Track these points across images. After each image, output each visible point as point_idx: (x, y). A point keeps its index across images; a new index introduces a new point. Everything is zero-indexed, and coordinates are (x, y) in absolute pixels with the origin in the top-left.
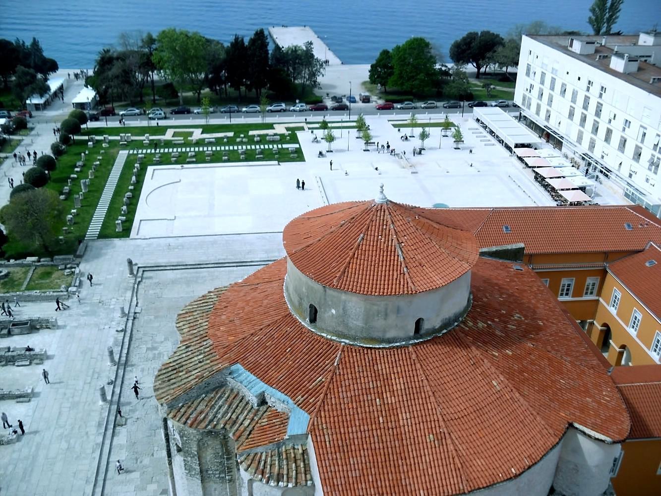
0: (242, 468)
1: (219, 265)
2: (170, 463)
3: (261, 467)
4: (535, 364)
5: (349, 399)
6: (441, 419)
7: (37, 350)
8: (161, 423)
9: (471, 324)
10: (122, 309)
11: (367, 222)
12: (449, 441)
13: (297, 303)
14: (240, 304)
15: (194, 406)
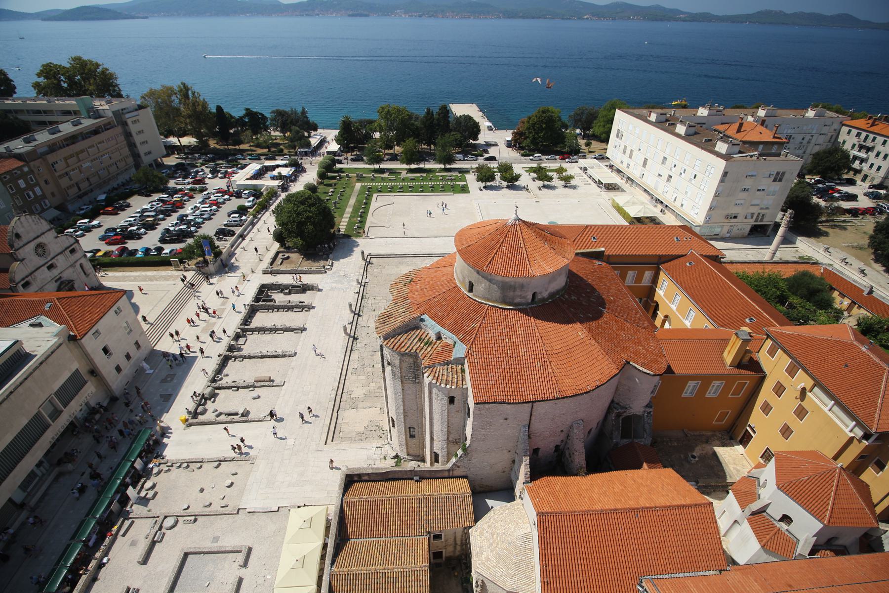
0: (426, 375)
1: (415, 256)
2: (384, 371)
3: (437, 375)
4: (607, 324)
6: (545, 353)
7: (306, 303)
9: (567, 297)
10: (357, 280)
12: (549, 367)
13: (461, 280)
14: (428, 280)
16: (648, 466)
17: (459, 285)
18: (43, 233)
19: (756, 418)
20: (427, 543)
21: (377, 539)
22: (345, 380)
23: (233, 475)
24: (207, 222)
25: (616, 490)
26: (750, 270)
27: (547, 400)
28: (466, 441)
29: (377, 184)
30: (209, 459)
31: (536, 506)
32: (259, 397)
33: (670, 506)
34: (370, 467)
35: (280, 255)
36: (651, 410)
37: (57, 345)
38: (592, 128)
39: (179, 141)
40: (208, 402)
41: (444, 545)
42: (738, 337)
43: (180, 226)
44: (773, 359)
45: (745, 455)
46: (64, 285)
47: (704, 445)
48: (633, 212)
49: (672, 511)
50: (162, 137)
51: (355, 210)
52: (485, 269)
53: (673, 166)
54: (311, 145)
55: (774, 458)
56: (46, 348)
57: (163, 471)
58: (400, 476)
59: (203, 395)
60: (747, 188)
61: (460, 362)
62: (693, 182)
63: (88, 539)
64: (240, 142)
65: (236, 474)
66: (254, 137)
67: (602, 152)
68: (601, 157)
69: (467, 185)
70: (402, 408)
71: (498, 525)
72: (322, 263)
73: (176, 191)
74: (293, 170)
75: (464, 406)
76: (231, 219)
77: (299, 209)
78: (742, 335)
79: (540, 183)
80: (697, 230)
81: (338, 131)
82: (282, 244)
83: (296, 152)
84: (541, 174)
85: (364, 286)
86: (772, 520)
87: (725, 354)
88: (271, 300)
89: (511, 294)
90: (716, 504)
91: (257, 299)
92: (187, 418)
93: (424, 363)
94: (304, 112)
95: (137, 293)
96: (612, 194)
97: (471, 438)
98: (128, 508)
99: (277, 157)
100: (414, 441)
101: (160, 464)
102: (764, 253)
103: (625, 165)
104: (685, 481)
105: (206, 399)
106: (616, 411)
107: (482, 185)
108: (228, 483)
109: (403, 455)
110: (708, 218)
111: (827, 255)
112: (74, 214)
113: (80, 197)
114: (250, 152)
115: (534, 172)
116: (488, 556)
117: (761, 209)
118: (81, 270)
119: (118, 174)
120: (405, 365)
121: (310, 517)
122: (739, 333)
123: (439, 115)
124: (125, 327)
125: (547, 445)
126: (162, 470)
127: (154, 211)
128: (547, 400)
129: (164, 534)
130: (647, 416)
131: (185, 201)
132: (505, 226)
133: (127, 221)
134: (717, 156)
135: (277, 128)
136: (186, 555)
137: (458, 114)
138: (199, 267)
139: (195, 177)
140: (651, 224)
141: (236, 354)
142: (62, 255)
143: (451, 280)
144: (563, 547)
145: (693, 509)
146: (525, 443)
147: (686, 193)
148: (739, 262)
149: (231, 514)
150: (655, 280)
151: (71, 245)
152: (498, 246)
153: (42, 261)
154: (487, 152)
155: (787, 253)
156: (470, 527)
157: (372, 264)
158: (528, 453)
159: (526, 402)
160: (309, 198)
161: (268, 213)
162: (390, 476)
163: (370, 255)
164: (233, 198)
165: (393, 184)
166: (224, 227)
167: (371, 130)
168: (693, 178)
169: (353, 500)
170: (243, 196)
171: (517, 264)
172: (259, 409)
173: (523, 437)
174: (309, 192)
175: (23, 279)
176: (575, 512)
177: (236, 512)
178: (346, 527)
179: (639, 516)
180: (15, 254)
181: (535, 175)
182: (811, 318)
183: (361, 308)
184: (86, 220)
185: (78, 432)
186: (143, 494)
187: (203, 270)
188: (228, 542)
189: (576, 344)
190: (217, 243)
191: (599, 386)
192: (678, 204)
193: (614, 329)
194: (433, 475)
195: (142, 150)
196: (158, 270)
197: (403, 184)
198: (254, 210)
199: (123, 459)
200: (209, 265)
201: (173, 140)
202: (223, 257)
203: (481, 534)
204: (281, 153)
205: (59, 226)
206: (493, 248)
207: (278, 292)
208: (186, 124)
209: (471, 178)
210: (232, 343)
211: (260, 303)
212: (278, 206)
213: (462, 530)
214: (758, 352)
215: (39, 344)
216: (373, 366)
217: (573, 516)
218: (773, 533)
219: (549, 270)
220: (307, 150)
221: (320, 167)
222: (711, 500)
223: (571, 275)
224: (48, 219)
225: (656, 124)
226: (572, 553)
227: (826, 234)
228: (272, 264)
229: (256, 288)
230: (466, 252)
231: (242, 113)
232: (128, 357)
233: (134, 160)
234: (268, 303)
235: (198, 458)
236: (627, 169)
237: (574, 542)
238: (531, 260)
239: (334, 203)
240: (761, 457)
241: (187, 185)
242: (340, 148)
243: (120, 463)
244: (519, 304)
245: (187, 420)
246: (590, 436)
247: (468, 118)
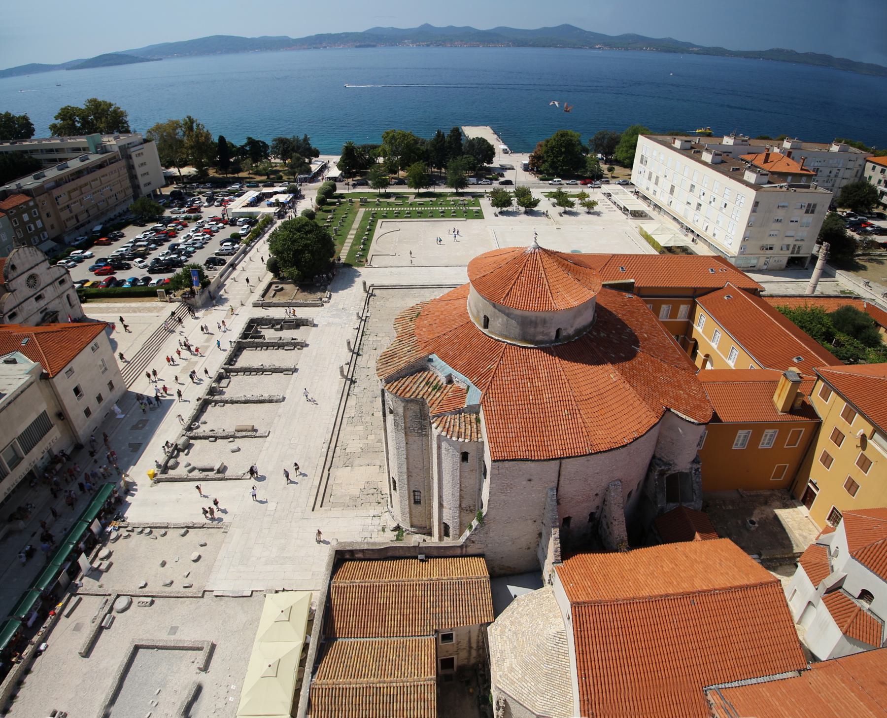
0: (434, 425)
1: (423, 287)
2: (385, 421)
4: (641, 365)
5: (509, 382)
6: (573, 400)
7: (299, 340)
8: (380, 393)
9: (595, 333)
10: (358, 314)
11: (525, 261)
12: (578, 416)
13: (475, 314)
14: (437, 314)
15: (402, 381)
16: (701, 536)
17: (473, 320)
18: (37, 265)
19: (817, 472)
20: (433, 646)
21: (371, 639)
22: (339, 430)
23: (202, 546)
24: (198, 251)
25: (666, 569)
26: (792, 305)
27: (578, 456)
28: (482, 508)
29: (382, 209)
30: (176, 524)
31: (569, 594)
32: (239, 450)
33: (731, 588)
34: (366, 541)
35: (273, 287)
36: (699, 466)
37: (28, 383)
38: (614, 153)
39: (179, 171)
40: (181, 454)
41: (455, 649)
42: (787, 378)
43: (171, 255)
44: (827, 403)
45: (810, 517)
46: (48, 316)
47: (763, 508)
48: (663, 241)
49: (734, 593)
50: (163, 168)
51: (358, 237)
52: (502, 302)
53: (702, 194)
54: (311, 171)
55: (842, 519)
56: (16, 387)
57: (122, 537)
58: (402, 553)
59: (176, 445)
60: (780, 218)
61: (474, 410)
62: (724, 211)
63: (28, 618)
64: (240, 170)
65: (205, 545)
66: (254, 165)
67: (626, 178)
68: (625, 183)
69: (481, 210)
71: (523, 620)
72: (319, 295)
73: (171, 220)
74: (291, 196)
75: (480, 464)
76: (223, 247)
77: (295, 236)
78: (791, 376)
79: (561, 209)
80: (732, 261)
81: (340, 156)
82: (276, 274)
83: (295, 179)
84: (562, 200)
85: (365, 321)
86: (850, 597)
87: (775, 398)
88: (260, 337)
89: (532, 330)
90: (784, 580)
91: (245, 336)
92: (156, 472)
93: (432, 411)
94: (306, 139)
95: (119, 327)
96: (639, 222)
97: (489, 505)
98: (77, 582)
99: (275, 184)
100: (419, 508)
101: (119, 527)
102: (803, 287)
103: (651, 191)
104: (745, 554)
105: (179, 451)
107: (498, 210)
108: (195, 556)
109: (405, 526)
110: (743, 248)
111: (868, 289)
112: (69, 245)
113: (77, 228)
114: (248, 180)
115: (554, 197)
116: (511, 665)
117: (797, 240)
118: (67, 301)
119: (117, 205)
121: (289, 606)
122: (787, 374)
123: (451, 137)
124: (100, 366)
125: (580, 513)
126: (121, 535)
127: (147, 240)
128: (578, 456)
129: (114, 618)
130: (695, 474)
131: (178, 230)
132: (523, 254)
133: (119, 251)
134: (747, 186)
135: (278, 155)
136: (137, 648)
137: (471, 137)
138: (185, 298)
139: (191, 205)
140: (683, 254)
141: (217, 398)
142: (51, 286)
143: (464, 314)
144: (606, 650)
145: (758, 590)
146: (553, 510)
147: (718, 222)
148: (780, 296)
149: (195, 597)
150: (691, 315)
151: (62, 276)
152: (517, 276)
153: (31, 292)
154: (502, 176)
155: (827, 287)
157: (375, 296)
158: (558, 524)
159: (553, 459)
160: (306, 224)
161: (261, 241)
162: (390, 554)
163: (372, 285)
164: (227, 226)
165: (400, 209)
166: (215, 256)
167: (375, 155)
168: (723, 206)
169: (343, 585)
170: (238, 223)
171: (538, 296)
172: (237, 465)
173: (551, 503)
174: (307, 219)
175: (11, 310)
176: (617, 600)
177: (200, 595)
178: (333, 622)
179: (696, 603)
180: (8, 285)
181: (555, 200)
182: (861, 356)
183: (361, 347)
184: (80, 251)
185: (36, 484)
186: (95, 565)
187: (189, 301)
188: (187, 636)
189: (608, 388)
190: (206, 273)
191: (637, 439)
192: (710, 233)
193: (651, 370)
194: (442, 552)
195: (142, 181)
196: (143, 301)
197: (411, 209)
198: (247, 238)
199: (79, 519)
200: (196, 296)
201: (174, 171)
202: (212, 288)
203: (502, 632)
204: (280, 180)
205: (53, 257)
206: (510, 279)
207: (269, 328)
208: (188, 155)
209: (485, 204)
210: (214, 385)
211: (248, 340)
212: (273, 234)
213: (478, 627)
214: (810, 395)
215: (10, 381)
216: (373, 414)
217: (616, 606)
218: (853, 615)
219: (575, 303)
220: (307, 176)
221: (319, 193)
222: (779, 577)
223: (599, 310)
224: (44, 250)
225: (682, 151)
226: (618, 658)
227: (864, 268)
228: (263, 296)
229: (245, 323)
230: (480, 283)
231: (244, 142)
232: (99, 399)
233: (134, 191)
234: (256, 340)
235: (163, 523)
236: (653, 196)
237: (619, 642)
238: (553, 291)
239: (335, 230)
240: (828, 519)
241: (181, 214)
242: (341, 174)
243: (75, 524)
244: (541, 342)
245: (155, 475)
246: (631, 501)
247: (482, 141)
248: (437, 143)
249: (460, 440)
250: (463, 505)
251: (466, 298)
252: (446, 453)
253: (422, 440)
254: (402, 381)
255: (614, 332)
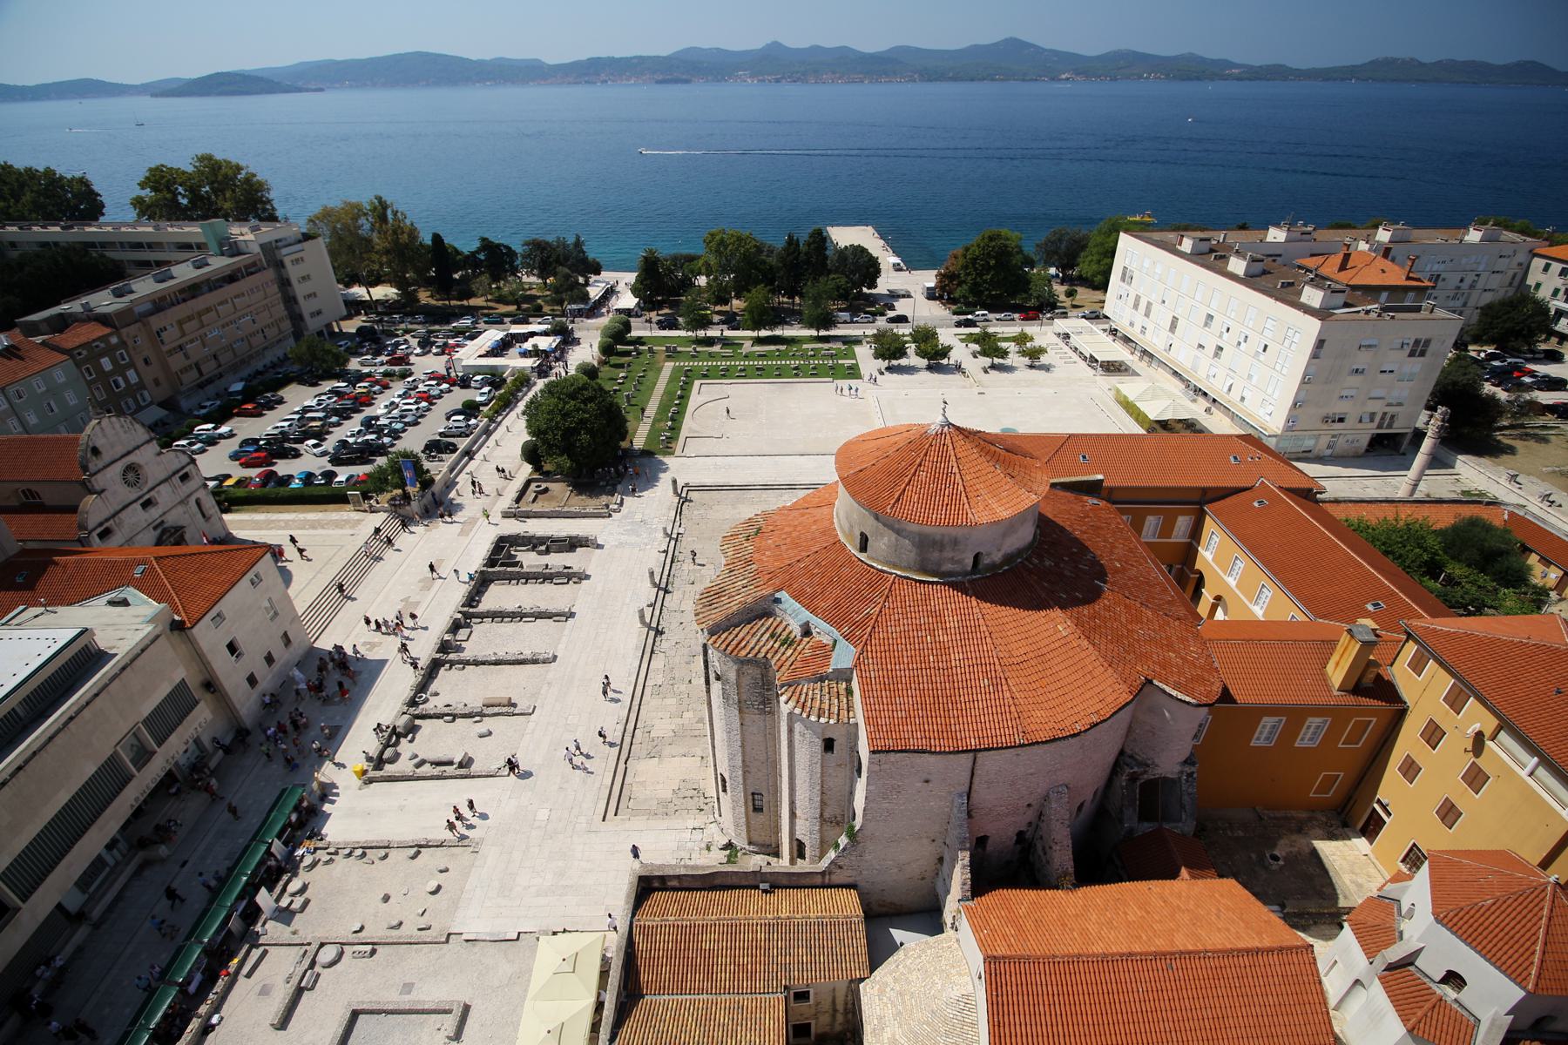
0: (783, 699)
1: (766, 487)
2: (708, 691)
3: (802, 700)
6: (997, 663)
7: (575, 569)
8: (701, 649)
9: (1036, 561)
10: (665, 529)
11: (926, 447)
12: (1005, 688)
13: (847, 530)
14: (787, 529)
15: (735, 632)
16: (1189, 873)
18: (138, 447)
19: (1391, 787)
20: (782, 1007)
21: (693, 997)
22: (640, 705)
23: (441, 871)
24: (410, 428)
25: (1131, 917)
26: (1371, 516)
27: (1002, 748)
28: (854, 819)
29: (700, 364)
30: (401, 843)
31: (982, 944)
32: (490, 733)
33: (1232, 950)
34: (682, 863)
35: (533, 486)
36: (1193, 769)
37: (151, 637)
38: (1078, 265)
39: (369, 292)
40: (402, 739)
41: (813, 1011)
42: (1352, 637)
43: (365, 435)
44: (1420, 679)
45: (1371, 856)
46: (168, 534)
47: (1294, 837)
48: (1154, 411)
49: (1236, 959)
50: (341, 286)
51: (663, 408)
52: (889, 511)
53: (1224, 330)
54: (589, 299)
55: (1427, 862)
56: (133, 643)
57: (321, 863)
58: (735, 881)
59: (394, 727)
60: (1361, 368)
61: (844, 676)
62: (1262, 357)
63: (188, 981)
64: (470, 295)
65: (446, 870)
66: (494, 286)
67: (1096, 307)
68: (1094, 315)
69: (857, 365)
70: (739, 758)
71: (913, 977)
72: (604, 499)
73: (361, 377)
74: (558, 341)
75: (851, 757)
76: (451, 423)
77: (567, 406)
78: (1360, 633)
79: (987, 361)
80: (1271, 443)
81: (636, 274)
82: (538, 468)
83: (563, 311)
84: (989, 347)
85: (677, 541)
86: (1426, 980)
87: (1330, 667)
88: (516, 564)
89: (935, 555)
90: (1320, 946)
91: (491, 562)
92: (365, 768)
93: (781, 677)
94: (578, 244)
95: (290, 552)
96: (1114, 380)
97: (864, 815)
98: (258, 928)
99: (531, 319)
100: (761, 818)
101: (316, 849)
102: (1396, 484)
103: (1137, 329)
104: (1259, 904)
105: (399, 736)
106: (1128, 770)
107: (883, 364)
108: (432, 886)
109: (741, 842)
110: (1291, 421)
111: (1514, 487)
112: (189, 414)
113: (201, 386)
114: (486, 311)
115: (976, 341)
116: (894, 1035)
117: (1389, 405)
118: (197, 510)
119: (266, 348)
120: (746, 680)
121: (574, 952)
122: (1354, 629)
123: (809, 244)
124: (266, 608)
125: (1002, 831)
126: (319, 860)
127: (323, 410)
128: (1002, 748)
129: (318, 975)
130: (1187, 781)
131: (375, 393)
132: (924, 435)
133: (277, 427)
134: (1305, 312)
135: (532, 270)
136: (355, 1014)
137: (842, 244)
138: (395, 505)
139: (393, 352)
140: (1188, 433)
141: (452, 656)
142: (166, 484)
143: (829, 531)
144: (1033, 1023)
145: (1275, 956)
146: (961, 826)
147: (1250, 377)
148: (1351, 501)
149: (436, 943)
150: (1196, 533)
151: (183, 468)
152: (913, 471)
153: (133, 494)
154: (892, 308)
155: (1439, 485)
156: (862, 980)
157: (691, 501)
158: (968, 845)
159: (963, 752)
160: (584, 387)
161: (513, 415)
162: (718, 882)
163: (687, 485)
164: (456, 389)
165: (728, 363)
166: (438, 438)
167: (692, 271)
168: (1261, 350)
169: (650, 923)
170: (473, 384)
171: (946, 502)
172: (488, 756)
173: (959, 815)
174: (585, 378)
175: (101, 524)
176: (1054, 956)
177: (444, 940)
178: (638, 973)
179: (1175, 968)
180: (90, 482)
181: (976, 347)
182: (1489, 602)
183: (671, 579)
184: (210, 426)
185: (178, 789)
186: (284, 903)
187: (401, 511)
188: (429, 993)
189: (1053, 646)
190: (426, 465)
191: (1097, 724)
192: (1235, 396)
194: (794, 881)
195: (306, 307)
196: (326, 511)
197: (747, 363)
198: (490, 409)
199: (253, 839)
200: (412, 503)
201: (359, 291)
202: (436, 488)
203: (882, 992)
204: (538, 312)
205: (165, 435)
206: (902, 475)
207: (528, 550)
208: (381, 265)
209: (864, 355)
210: (447, 637)
211: (497, 569)
212: (532, 402)
213: (847, 984)
214: (1392, 665)
215: (120, 634)
216: (690, 681)
217: (1051, 964)
218: (1428, 1005)
219: (1004, 513)
220: (582, 306)
221: (604, 334)
222: (1310, 940)
223: (1044, 524)
224: (147, 423)
225: (1194, 258)
226: (1050, 1035)
227: (1511, 450)
228: (518, 500)
229: (490, 542)
230: (854, 482)
231: (475, 245)
232: (269, 659)
233: (294, 325)
234: (509, 569)
235: (382, 841)
236: (1141, 336)
237: (1053, 1013)
238: (970, 495)
239: (628, 396)
240: (1403, 861)
241: (378, 366)
242: (638, 304)
243: (247, 847)
244: (950, 574)
245: (365, 772)
246: (1082, 816)
247: (860, 251)
248: (788, 255)
249: (823, 720)
250: (826, 815)
251: (832, 504)
252: (801, 739)
253: (765, 720)
254: (735, 632)
255: (1066, 559)
